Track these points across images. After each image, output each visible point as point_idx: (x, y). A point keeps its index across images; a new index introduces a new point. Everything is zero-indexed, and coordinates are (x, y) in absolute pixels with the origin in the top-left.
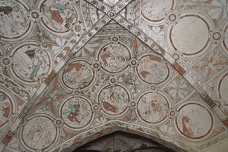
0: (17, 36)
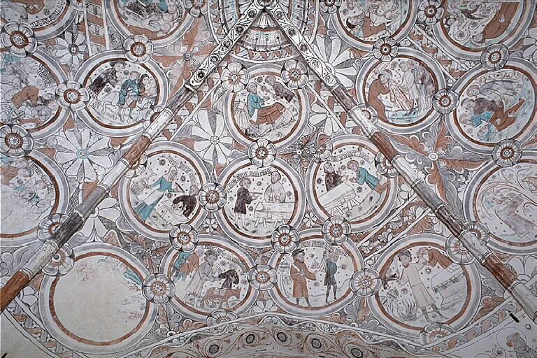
0: (293, 196)
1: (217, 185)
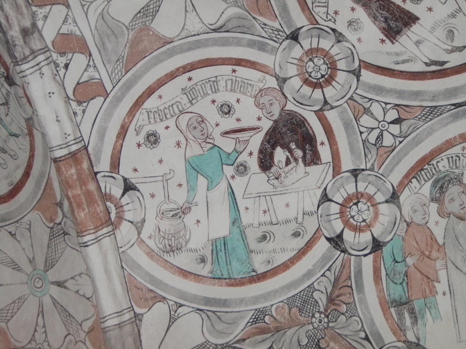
1: (294, 37)
